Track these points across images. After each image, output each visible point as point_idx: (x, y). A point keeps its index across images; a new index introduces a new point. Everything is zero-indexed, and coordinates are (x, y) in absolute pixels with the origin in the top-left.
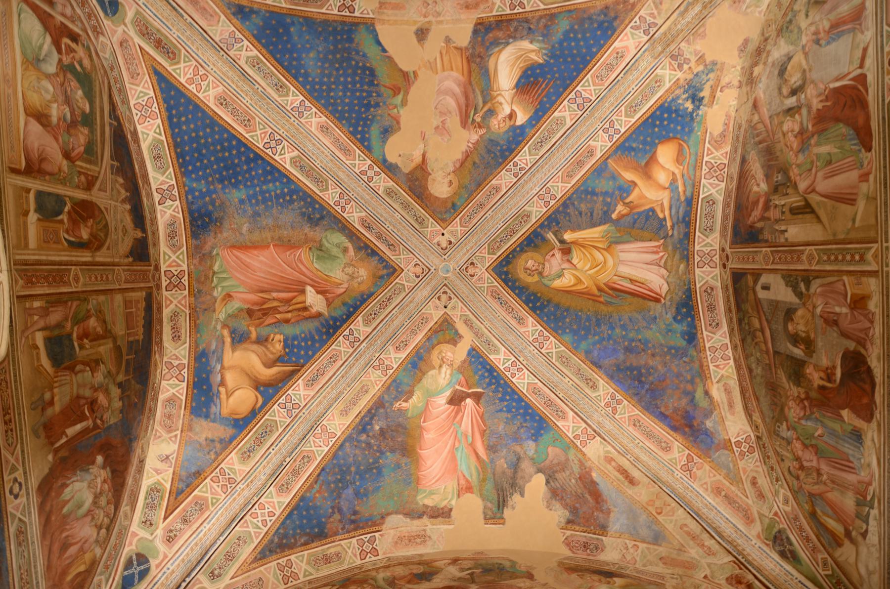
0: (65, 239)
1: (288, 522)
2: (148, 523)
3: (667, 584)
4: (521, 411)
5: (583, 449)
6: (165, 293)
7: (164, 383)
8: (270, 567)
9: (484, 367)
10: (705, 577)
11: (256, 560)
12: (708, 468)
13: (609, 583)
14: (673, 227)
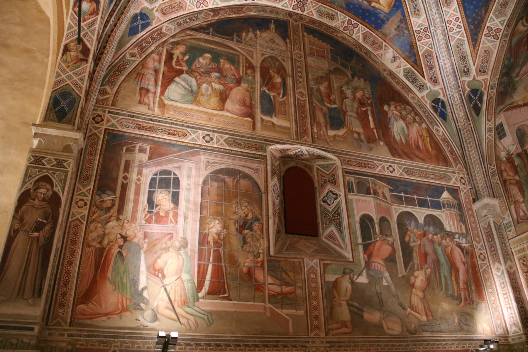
0: (283, 97)
1: (468, 12)
2: (421, 87)
6: (305, 14)
7: (354, 36)
8: (484, 41)
11: (474, 46)
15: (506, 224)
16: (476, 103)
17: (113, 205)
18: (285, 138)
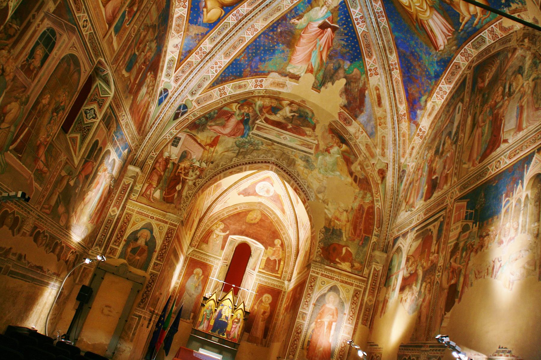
2: (168, 75)
3: (359, 158)
4: (353, 44)
5: (369, 78)
7: (176, 9)
8: (215, 90)
9: (345, 14)
10: (373, 164)
11: (210, 87)
12: (407, 124)
13: (340, 146)
14: (462, 30)
15: (135, 190)
16: (180, 113)
17: (14, 35)
18: (109, 57)
